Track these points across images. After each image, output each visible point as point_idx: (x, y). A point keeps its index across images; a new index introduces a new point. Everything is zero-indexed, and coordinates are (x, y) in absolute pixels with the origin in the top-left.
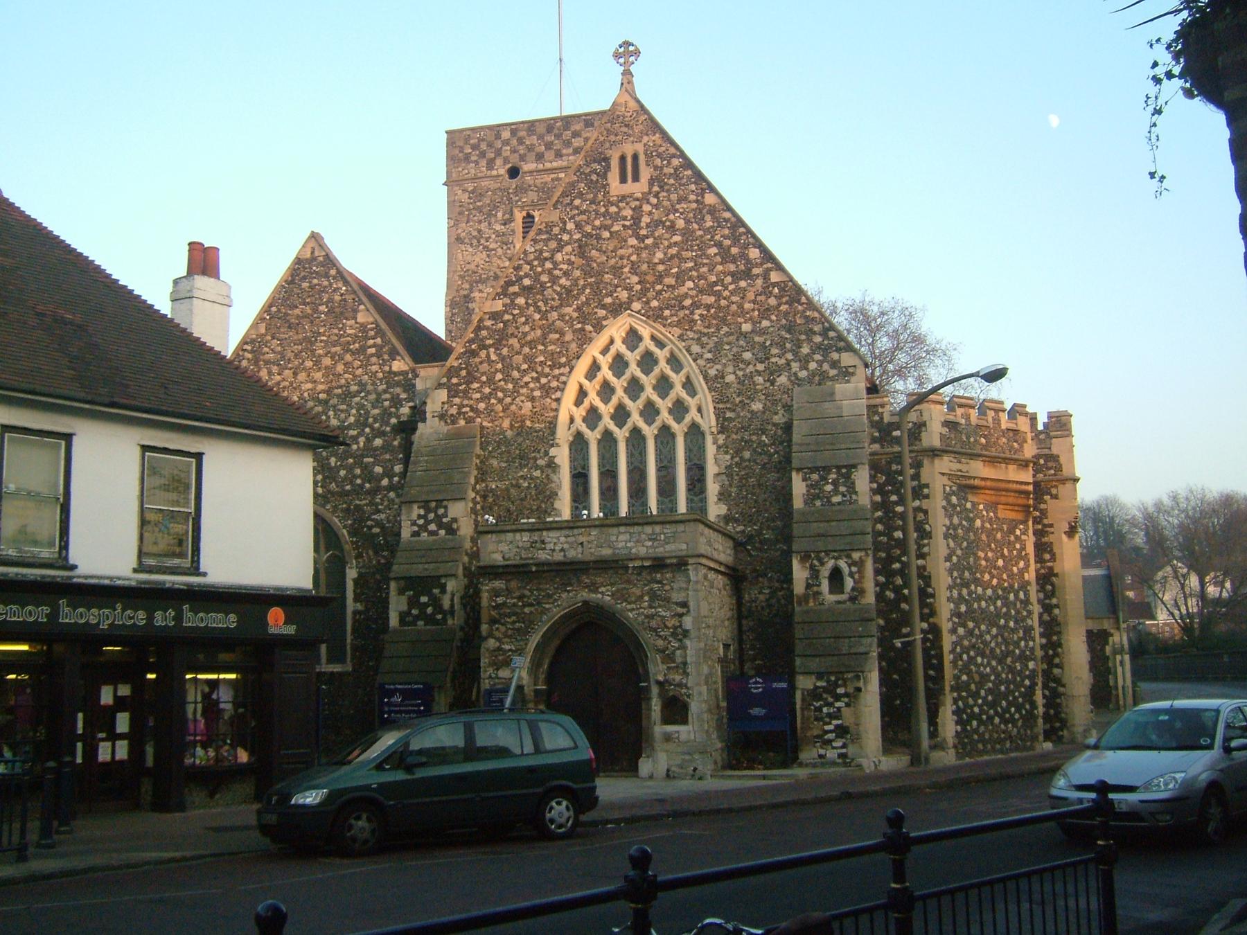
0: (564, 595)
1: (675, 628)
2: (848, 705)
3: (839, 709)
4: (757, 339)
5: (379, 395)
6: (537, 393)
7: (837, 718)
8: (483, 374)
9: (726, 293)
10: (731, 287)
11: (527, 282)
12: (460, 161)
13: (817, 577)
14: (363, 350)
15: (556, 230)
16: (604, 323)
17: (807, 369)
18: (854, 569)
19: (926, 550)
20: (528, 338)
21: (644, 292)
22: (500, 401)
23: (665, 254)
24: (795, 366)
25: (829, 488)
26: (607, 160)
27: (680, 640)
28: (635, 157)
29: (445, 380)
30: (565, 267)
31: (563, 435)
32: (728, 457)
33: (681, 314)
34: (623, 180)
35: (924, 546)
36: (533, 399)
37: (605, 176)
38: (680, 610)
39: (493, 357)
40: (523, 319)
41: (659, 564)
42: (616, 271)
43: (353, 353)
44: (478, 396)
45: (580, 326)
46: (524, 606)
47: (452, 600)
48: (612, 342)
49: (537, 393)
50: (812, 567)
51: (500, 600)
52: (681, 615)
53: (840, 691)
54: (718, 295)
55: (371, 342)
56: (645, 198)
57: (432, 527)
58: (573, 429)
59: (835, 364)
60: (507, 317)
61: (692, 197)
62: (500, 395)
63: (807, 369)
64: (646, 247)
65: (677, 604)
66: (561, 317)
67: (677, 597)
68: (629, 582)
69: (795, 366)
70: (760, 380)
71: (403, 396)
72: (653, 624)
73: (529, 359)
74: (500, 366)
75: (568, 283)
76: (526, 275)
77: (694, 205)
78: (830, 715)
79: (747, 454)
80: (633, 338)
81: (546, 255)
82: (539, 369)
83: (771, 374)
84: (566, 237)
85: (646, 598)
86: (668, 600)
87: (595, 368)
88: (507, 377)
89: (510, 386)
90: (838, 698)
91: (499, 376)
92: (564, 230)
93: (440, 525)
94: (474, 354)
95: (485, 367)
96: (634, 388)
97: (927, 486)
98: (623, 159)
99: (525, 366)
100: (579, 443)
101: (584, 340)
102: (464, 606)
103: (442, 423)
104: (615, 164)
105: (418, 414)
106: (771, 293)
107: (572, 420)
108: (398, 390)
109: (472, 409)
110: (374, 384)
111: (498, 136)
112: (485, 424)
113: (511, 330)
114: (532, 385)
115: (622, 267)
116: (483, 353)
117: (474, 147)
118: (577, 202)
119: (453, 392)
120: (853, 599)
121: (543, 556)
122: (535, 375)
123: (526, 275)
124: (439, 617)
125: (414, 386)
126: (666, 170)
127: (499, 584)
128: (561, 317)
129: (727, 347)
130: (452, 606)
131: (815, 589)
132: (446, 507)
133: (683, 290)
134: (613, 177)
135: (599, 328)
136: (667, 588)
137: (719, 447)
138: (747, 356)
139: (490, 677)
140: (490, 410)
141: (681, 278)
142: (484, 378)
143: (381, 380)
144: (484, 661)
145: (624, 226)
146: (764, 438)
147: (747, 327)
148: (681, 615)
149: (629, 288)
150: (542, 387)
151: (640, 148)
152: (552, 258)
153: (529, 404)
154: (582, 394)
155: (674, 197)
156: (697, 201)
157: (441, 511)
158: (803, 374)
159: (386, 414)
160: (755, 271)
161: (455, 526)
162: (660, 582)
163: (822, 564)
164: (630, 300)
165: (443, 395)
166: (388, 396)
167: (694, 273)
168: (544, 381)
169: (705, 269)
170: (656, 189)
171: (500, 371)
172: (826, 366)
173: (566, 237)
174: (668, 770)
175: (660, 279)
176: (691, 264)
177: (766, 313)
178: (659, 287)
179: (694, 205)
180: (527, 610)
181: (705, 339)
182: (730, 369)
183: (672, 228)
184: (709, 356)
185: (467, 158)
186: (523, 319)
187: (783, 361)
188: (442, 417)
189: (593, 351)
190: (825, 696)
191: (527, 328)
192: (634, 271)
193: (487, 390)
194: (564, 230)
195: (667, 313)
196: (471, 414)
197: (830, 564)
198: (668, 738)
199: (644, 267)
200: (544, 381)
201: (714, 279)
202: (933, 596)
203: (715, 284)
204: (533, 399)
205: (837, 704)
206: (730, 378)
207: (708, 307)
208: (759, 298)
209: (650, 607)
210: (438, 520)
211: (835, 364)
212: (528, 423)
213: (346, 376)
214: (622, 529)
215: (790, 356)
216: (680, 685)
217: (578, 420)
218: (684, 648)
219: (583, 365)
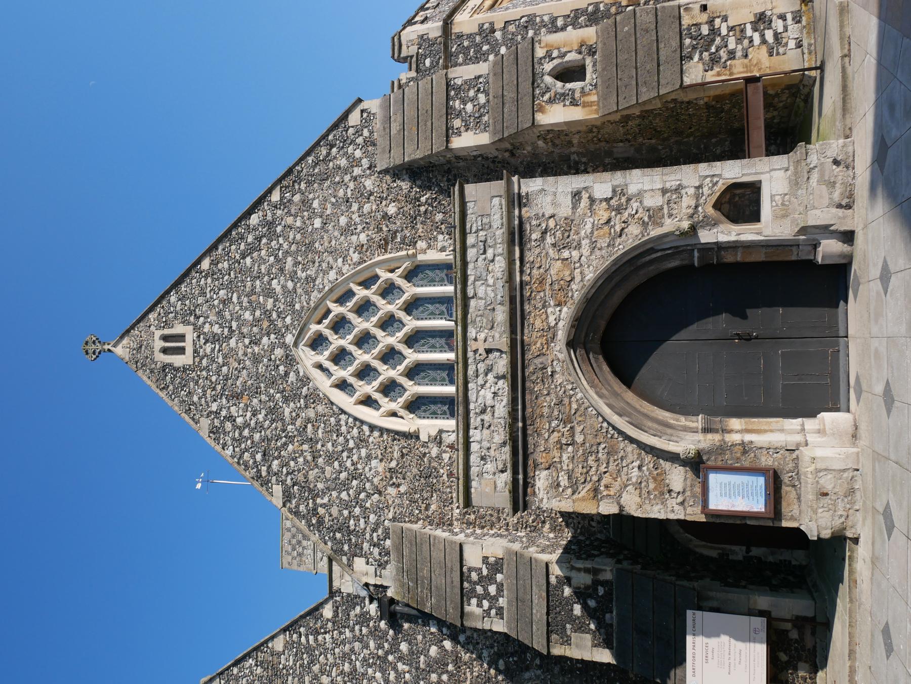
0: (559, 378)
1: (610, 208)
2: (725, 19)
3: (731, 29)
4: (328, 212)
5: (355, 639)
6: (363, 452)
7: (743, 31)
8: (342, 515)
9: (285, 246)
10: (281, 240)
11: (259, 457)
12: (301, 561)
13: (563, 94)
14: (309, 650)
15: (217, 423)
16: (301, 374)
17: (361, 159)
18: (555, 54)
19: (546, 18)
20: (309, 458)
21: (277, 332)
22: (369, 496)
23: (246, 309)
24: (357, 171)
25: (469, 107)
26: (165, 367)
27: (629, 200)
28: (165, 338)
29: (344, 559)
30: (249, 414)
31: (408, 423)
32: (440, 237)
33: (299, 291)
34: (182, 351)
35: (543, 21)
36: (369, 457)
37: (177, 369)
38: (585, 202)
39: (326, 500)
40: (292, 463)
41: (517, 236)
42: (256, 360)
43: (312, 662)
44: (362, 521)
45: (302, 401)
46: (573, 443)
47: (579, 570)
48: (320, 367)
49: (363, 452)
50: (551, 101)
51: (564, 481)
52: (592, 200)
53: (705, 30)
54: (287, 253)
55: (303, 639)
56: (197, 328)
57: (492, 589)
58: (402, 412)
59: (358, 133)
60: (289, 482)
61: (203, 282)
62: (362, 496)
63: (361, 159)
64: (239, 327)
65: (574, 207)
66: (293, 421)
67: (565, 210)
68: (542, 281)
69: (357, 171)
70: (367, 208)
71: (358, 609)
72: (603, 242)
73: (331, 458)
74: (335, 494)
75: (263, 412)
76: (253, 456)
77: (209, 280)
78: (739, 41)
79: (439, 217)
80: (318, 342)
81: (237, 435)
82: (340, 448)
83: (363, 196)
84: (224, 413)
85: (566, 254)
86: (569, 221)
87: (342, 385)
88: (345, 486)
89: (355, 483)
90: (714, 32)
91: (344, 495)
92: (217, 413)
93: (491, 579)
94: (321, 522)
95: (335, 511)
96: (365, 339)
97: (481, 26)
98: (165, 351)
99: (336, 464)
100: (416, 405)
101: (314, 397)
102: (590, 557)
103: (388, 566)
104: (168, 359)
105: (376, 593)
106: (289, 201)
107: (394, 414)
108: (352, 613)
109: (374, 530)
110: (343, 642)
111: (289, 530)
112: (390, 516)
113: (300, 477)
114: (355, 458)
115: (253, 354)
116: (321, 511)
117: (294, 549)
118: (195, 399)
119: (357, 551)
120: (592, 52)
121: (502, 409)
122: (345, 454)
123: (253, 456)
124: (601, 591)
125: (349, 595)
126: (178, 308)
127: (541, 480)
128: (293, 421)
129: (333, 242)
130: (587, 571)
131: (577, 95)
132: (470, 570)
133: (278, 289)
134: (178, 361)
135: (305, 380)
136: (552, 223)
137: (429, 247)
138: (343, 220)
139: (682, 503)
140: (379, 509)
141: (269, 293)
142: (346, 513)
143: (341, 633)
144: (656, 512)
145: (219, 351)
146: (423, 199)
147: (318, 223)
148: (592, 200)
149: (272, 348)
150: (358, 447)
151: (158, 334)
152: (239, 428)
153: (374, 463)
154: (368, 401)
155: (201, 300)
156: (206, 277)
157: (474, 576)
158: (365, 163)
159: (375, 633)
160: (269, 218)
161: (492, 560)
162: (544, 233)
163: (548, 89)
164: (284, 346)
165: (359, 563)
166: (357, 628)
167: (266, 279)
168: (351, 444)
169: (263, 267)
170: (192, 319)
171: (340, 493)
172: (360, 140)
173: (224, 413)
174: (840, 206)
175: (267, 314)
176: (258, 282)
177: (306, 203)
178: (274, 315)
179: (209, 280)
180: (579, 438)
181: (324, 265)
182: (354, 238)
183: (226, 302)
184: (340, 260)
185: (300, 555)
186: (292, 463)
187: (352, 185)
188: (382, 565)
189: (324, 384)
190: (713, 49)
191: (301, 460)
192: (256, 342)
193: (357, 511)
194: (217, 413)
195: (297, 307)
196: (380, 531)
197: (548, 79)
198: (783, 213)
199: (255, 329)
200: (351, 444)
201: (272, 258)
202: (597, 5)
203: (276, 256)
204: (369, 457)
205: (724, 31)
206: (363, 238)
207: (296, 264)
208: (293, 211)
209: (579, 246)
210: (485, 580)
211: (358, 133)
212: (393, 464)
213: (334, 674)
214: (470, 292)
215: (347, 178)
216: (697, 197)
217: (393, 406)
218: (640, 195)
219: (340, 398)
